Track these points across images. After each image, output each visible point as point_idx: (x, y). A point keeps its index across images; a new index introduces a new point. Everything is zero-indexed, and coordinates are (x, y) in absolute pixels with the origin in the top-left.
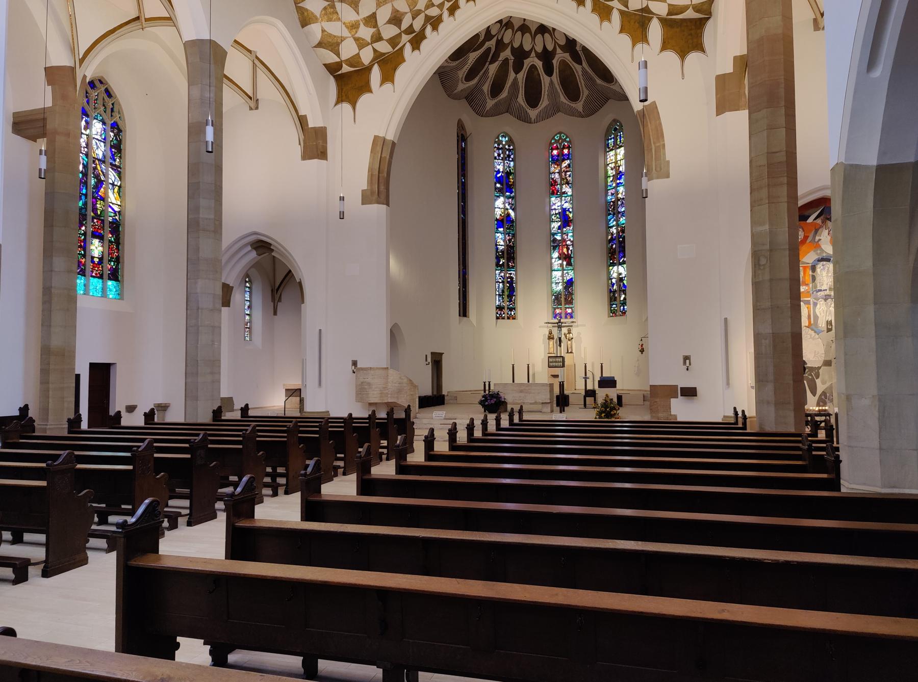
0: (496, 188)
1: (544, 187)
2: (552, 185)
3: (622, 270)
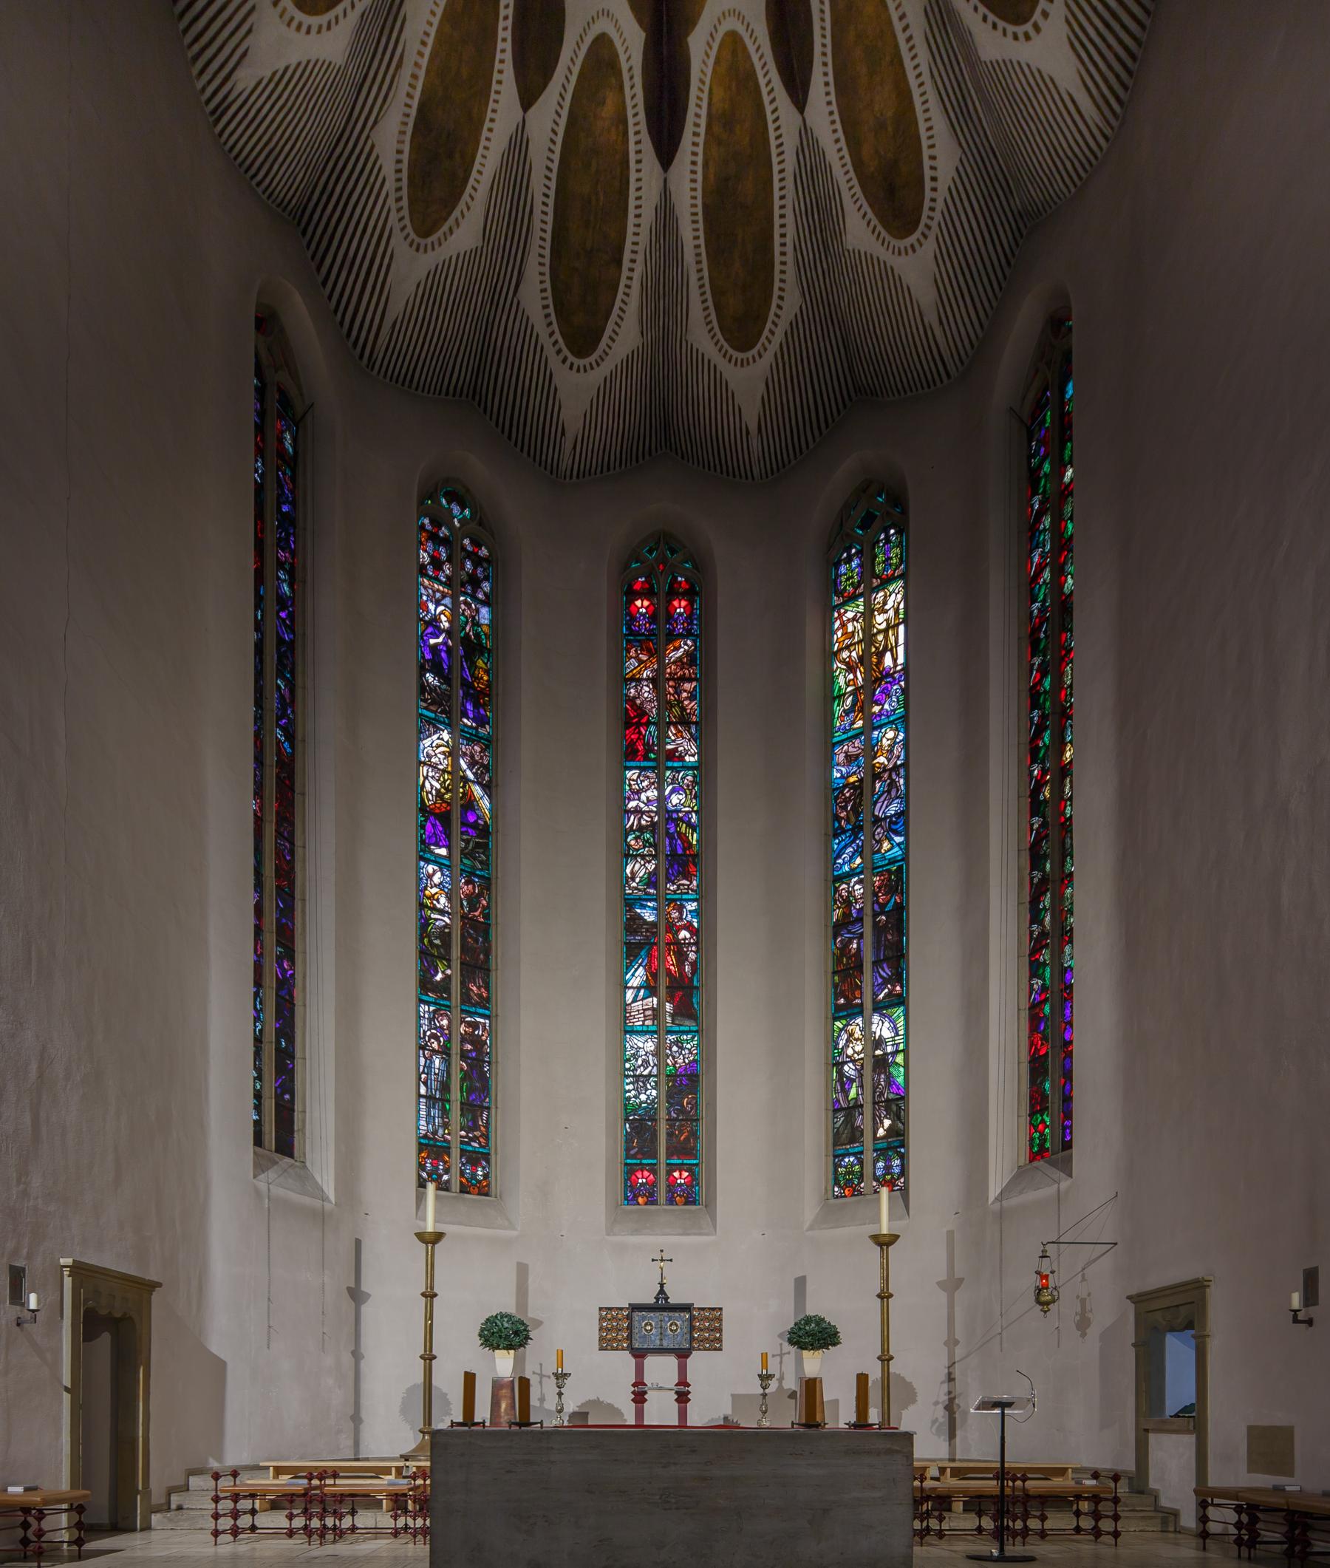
0: (423, 688)
1: (601, 732)
2: (628, 724)
3: (882, 1029)
